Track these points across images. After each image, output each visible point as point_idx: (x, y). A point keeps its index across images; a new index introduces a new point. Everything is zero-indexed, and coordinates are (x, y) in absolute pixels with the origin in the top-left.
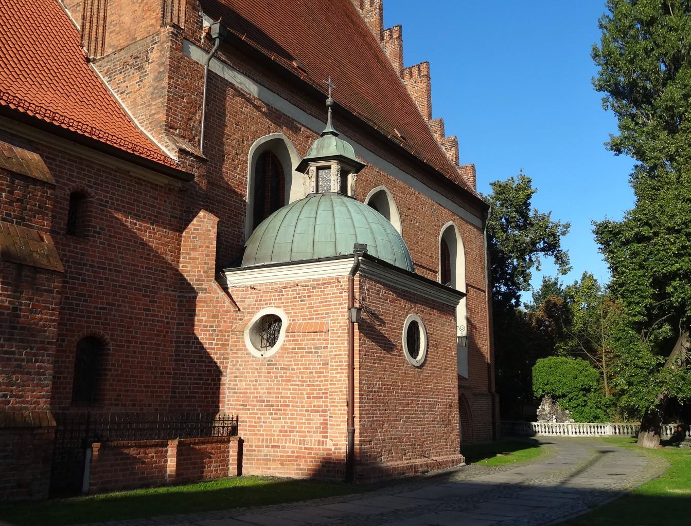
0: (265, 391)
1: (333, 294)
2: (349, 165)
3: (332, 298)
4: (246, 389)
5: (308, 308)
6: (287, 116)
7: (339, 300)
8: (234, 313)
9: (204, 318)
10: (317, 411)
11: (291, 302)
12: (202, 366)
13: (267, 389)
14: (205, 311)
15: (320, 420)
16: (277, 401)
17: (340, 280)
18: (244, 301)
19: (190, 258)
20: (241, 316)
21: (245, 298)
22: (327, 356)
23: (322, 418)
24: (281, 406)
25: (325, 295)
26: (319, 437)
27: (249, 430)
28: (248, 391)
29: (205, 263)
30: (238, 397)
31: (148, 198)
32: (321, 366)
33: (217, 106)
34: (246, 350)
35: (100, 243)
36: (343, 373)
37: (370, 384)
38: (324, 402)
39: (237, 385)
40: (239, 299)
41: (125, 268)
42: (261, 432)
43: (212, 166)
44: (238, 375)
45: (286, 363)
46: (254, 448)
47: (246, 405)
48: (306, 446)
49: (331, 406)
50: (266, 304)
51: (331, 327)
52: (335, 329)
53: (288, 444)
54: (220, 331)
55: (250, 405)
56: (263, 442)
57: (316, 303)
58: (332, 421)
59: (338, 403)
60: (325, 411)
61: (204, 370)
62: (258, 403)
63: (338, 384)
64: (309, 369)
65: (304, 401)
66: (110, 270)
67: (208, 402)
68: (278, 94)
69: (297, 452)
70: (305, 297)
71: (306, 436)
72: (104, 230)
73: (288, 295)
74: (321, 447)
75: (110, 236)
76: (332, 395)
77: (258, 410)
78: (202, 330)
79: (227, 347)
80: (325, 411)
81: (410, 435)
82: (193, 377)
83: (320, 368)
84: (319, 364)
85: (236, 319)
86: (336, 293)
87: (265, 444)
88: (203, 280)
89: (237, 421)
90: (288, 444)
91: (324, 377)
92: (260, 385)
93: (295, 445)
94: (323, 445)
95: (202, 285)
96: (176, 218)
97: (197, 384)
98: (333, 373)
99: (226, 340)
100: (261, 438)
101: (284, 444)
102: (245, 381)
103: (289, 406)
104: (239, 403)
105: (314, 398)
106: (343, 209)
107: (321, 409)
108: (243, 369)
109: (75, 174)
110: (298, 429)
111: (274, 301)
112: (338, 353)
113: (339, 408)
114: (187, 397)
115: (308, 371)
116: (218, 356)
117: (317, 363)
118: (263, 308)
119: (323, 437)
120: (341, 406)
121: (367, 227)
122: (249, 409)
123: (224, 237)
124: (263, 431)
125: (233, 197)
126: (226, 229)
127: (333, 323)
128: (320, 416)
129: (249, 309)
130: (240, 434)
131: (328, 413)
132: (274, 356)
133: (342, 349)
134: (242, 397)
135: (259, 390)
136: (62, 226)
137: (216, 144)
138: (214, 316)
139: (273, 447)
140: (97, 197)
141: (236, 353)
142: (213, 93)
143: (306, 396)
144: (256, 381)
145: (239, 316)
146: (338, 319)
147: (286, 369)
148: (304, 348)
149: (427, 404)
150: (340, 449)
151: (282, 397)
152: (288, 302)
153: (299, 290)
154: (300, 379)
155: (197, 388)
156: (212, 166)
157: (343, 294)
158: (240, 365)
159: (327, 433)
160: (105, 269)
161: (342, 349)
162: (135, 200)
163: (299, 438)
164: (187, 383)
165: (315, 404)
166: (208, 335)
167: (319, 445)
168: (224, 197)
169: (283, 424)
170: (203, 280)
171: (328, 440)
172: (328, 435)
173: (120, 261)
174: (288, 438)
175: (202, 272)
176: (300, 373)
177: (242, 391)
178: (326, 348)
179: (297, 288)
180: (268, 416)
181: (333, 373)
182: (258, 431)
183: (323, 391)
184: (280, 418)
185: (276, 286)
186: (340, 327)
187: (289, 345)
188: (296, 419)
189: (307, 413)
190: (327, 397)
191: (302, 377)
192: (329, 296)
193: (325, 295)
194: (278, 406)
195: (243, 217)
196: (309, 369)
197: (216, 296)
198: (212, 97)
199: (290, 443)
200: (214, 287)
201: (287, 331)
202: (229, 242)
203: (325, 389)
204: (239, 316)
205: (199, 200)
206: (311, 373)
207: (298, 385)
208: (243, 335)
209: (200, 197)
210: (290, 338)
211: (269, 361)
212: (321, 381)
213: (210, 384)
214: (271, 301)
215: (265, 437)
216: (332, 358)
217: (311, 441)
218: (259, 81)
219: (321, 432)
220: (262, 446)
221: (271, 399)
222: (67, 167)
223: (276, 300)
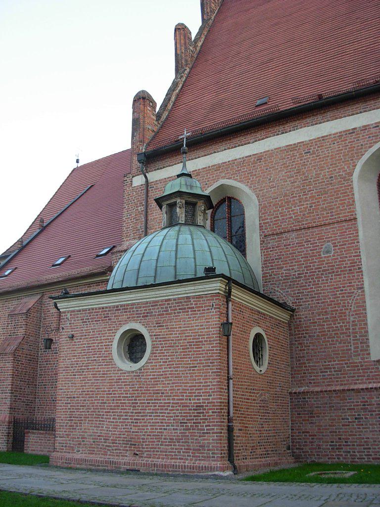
37: (68, 392)
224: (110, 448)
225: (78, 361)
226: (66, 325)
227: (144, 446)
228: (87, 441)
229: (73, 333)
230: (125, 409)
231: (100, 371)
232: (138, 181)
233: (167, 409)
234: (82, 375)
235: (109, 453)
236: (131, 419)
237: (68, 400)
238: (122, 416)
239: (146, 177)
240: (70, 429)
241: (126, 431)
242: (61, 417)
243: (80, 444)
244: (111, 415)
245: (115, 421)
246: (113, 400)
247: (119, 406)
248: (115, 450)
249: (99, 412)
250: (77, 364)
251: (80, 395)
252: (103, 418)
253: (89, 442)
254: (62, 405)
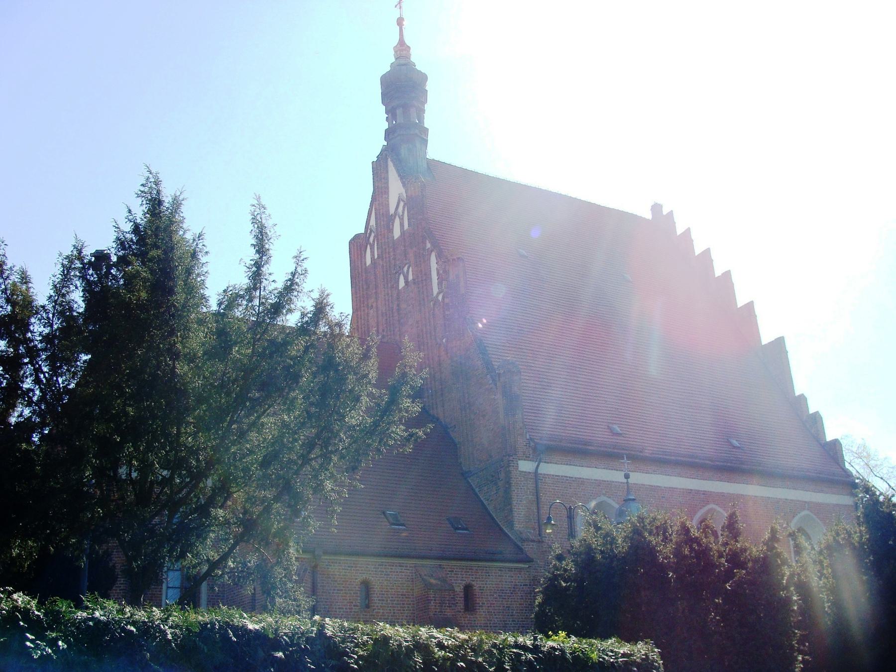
31: (507, 577)
33: (548, 497)
35: (483, 612)
41: (499, 624)
66: (491, 627)
68: (596, 467)
72: (484, 604)
75: (488, 607)
96: (526, 585)
109: (464, 576)
136: (462, 607)
140: (478, 586)
142: (544, 488)
160: (488, 626)
162: (500, 582)
173: (496, 620)
222: (460, 573)
232: (525, 466)
239: (538, 466)
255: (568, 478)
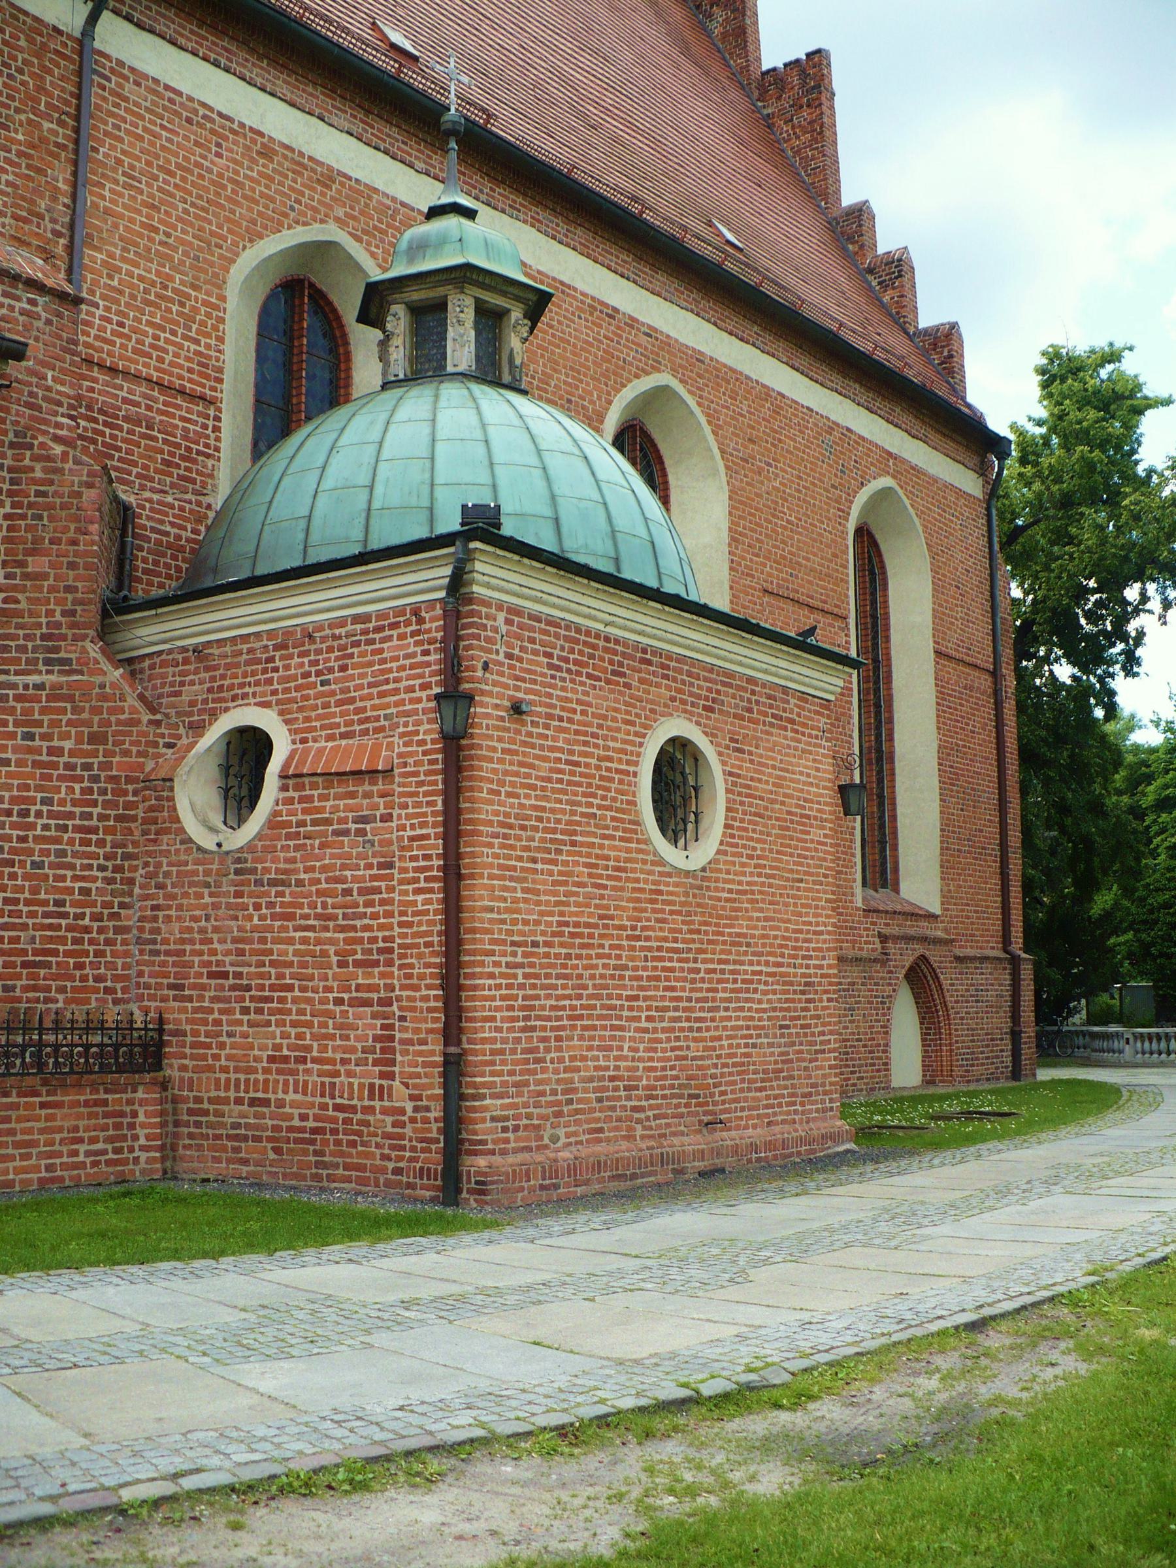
0: (230, 946)
1: (406, 657)
2: (504, 294)
3: (402, 668)
4: (183, 941)
5: (339, 703)
6: (350, 178)
7: (422, 676)
8: (151, 729)
9: (68, 745)
10: (367, 1003)
11: (297, 688)
12: (63, 878)
13: (235, 941)
14: (70, 723)
15: (374, 1027)
16: (261, 976)
17: (423, 614)
18: (178, 694)
19: (26, 576)
20: (170, 736)
21: (182, 684)
22: (390, 843)
23: (379, 1023)
24: (272, 988)
25: (383, 661)
26: (371, 1074)
27: (193, 1057)
28: (188, 947)
29: (69, 589)
30: (164, 964)
32: (375, 871)
33: (124, 152)
34: (182, 830)
36: (431, 890)
37: (514, 922)
38: (382, 975)
39: (157, 931)
40: (167, 689)
42: (223, 1062)
43: (109, 321)
44: (161, 902)
45: (282, 866)
46: (206, 1106)
47: (180, 987)
48: (338, 1101)
49: (403, 987)
50: (234, 698)
51: (400, 755)
52: (411, 761)
53: (292, 1096)
54: (114, 779)
55: (194, 987)
56: (227, 1089)
57: (361, 687)
58: (406, 1029)
59: (422, 977)
60: (388, 1002)
61: (70, 890)
62: (213, 982)
63: (420, 923)
64: (343, 880)
65: (330, 973)
67: (84, 978)
68: (322, 119)
69: (317, 1118)
70: (331, 670)
71: (337, 1074)
73: (287, 667)
74: (377, 1104)
76: (404, 956)
77: (214, 999)
78: (61, 778)
79: (132, 825)
80: (388, 1002)
81: (664, 1069)
82: (40, 909)
83: (373, 878)
84: (369, 866)
85: (155, 745)
86: (414, 655)
87: (232, 1094)
88: (63, 638)
89: (161, 1031)
90: (292, 1096)
91: (383, 902)
92: (216, 930)
93: (309, 1099)
94: (381, 1099)
95: (57, 650)
97: (50, 927)
98: (406, 893)
99: (129, 806)
100: (223, 1076)
101: (280, 1095)
102: (179, 918)
103: (290, 988)
104: (165, 981)
105: (357, 964)
106: (468, 417)
107: (375, 996)
108: (174, 886)
110: (315, 1054)
111: (251, 690)
112: (419, 832)
113: (424, 992)
114: (25, 965)
115: (340, 886)
116: (108, 849)
117: (362, 863)
118: (227, 710)
119: (382, 1075)
120: (428, 987)
121: (534, 461)
122: (190, 999)
123: (149, 518)
124: (229, 1058)
125: (179, 407)
126: (156, 497)
127: (406, 744)
128: (374, 1016)
129: (191, 714)
130: (171, 1066)
131: (395, 1008)
132: (250, 847)
133: (430, 819)
134: (174, 964)
135: (216, 945)
137: (124, 259)
138: (94, 738)
139: (253, 1102)
141: (155, 841)
143: (335, 959)
144: (208, 919)
145: (163, 736)
146: (417, 733)
147: (283, 883)
148: (327, 822)
149: (727, 981)
150: (428, 1109)
151: (273, 963)
152: (287, 690)
153: (318, 652)
154: (319, 910)
155: (51, 939)
156: (109, 321)
157: (432, 658)
158: (167, 874)
159: (393, 1063)
161: (430, 819)
163: (319, 1080)
164: (25, 927)
165: (360, 981)
166: (77, 791)
167: (371, 1097)
168: (149, 408)
169: (278, 1041)
170: (63, 638)
171: (396, 1084)
172: (397, 1069)
174: (291, 1079)
175: (58, 614)
176: (319, 893)
177: (172, 947)
178: (387, 818)
179: (313, 647)
180: (238, 1016)
181: (406, 893)
182: (216, 1057)
183: (381, 944)
184: (268, 1024)
185: (257, 645)
186: (425, 753)
187: (291, 813)
188: (309, 1025)
189: (338, 1009)
190: (390, 963)
191: (324, 906)
192: (394, 665)
193: (383, 661)
194: (262, 988)
195: (210, 462)
196: (343, 880)
197: (97, 679)
198: (109, 128)
199: (296, 1091)
200: (93, 654)
201: (283, 776)
202: (167, 534)
203: (385, 939)
204: (163, 736)
205: (56, 414)
206: (347, 892)
207: (311, 928)
208: (172, 789)
209: (60, 404)
210: (291, 793)
211: (238, 861)
212: (375, 916)
213: (87, 930)
214: (247, 689)
215: (233, 1076)
216: (402, 849)
217: (351, 1085)
218: (259, 81)
219: (376, 1063)
220: (226, 1101)
221: (245, 970)
223: (257, 683)
224: (642, 1116)
225: (543, 809)
226: (494, 656)
227: (717, 1098)
228: (580, 1101)
229: (520, 695)
230: (673, 989)
231: (608, 858)
233: (755, 991)
234: (554, 862)
235: (639, 1131)
236: (688, 1019)
237: (514, 954)
238: (666, 1009)
240: (527, 1061)
241: (678, 1058)
242: (493, 1019)
243: (559, 1114)
244: (640, 1009)
245: (649, 1025)
246: (646, 959)
247: (658, 979)
248: (656, 1117)
249: (610, 997)
250: (539, 819)
251: (554, 934)
252: (620, 1018)
253: (588, 1101)
254: (497, 971)
255: (215, 116)
